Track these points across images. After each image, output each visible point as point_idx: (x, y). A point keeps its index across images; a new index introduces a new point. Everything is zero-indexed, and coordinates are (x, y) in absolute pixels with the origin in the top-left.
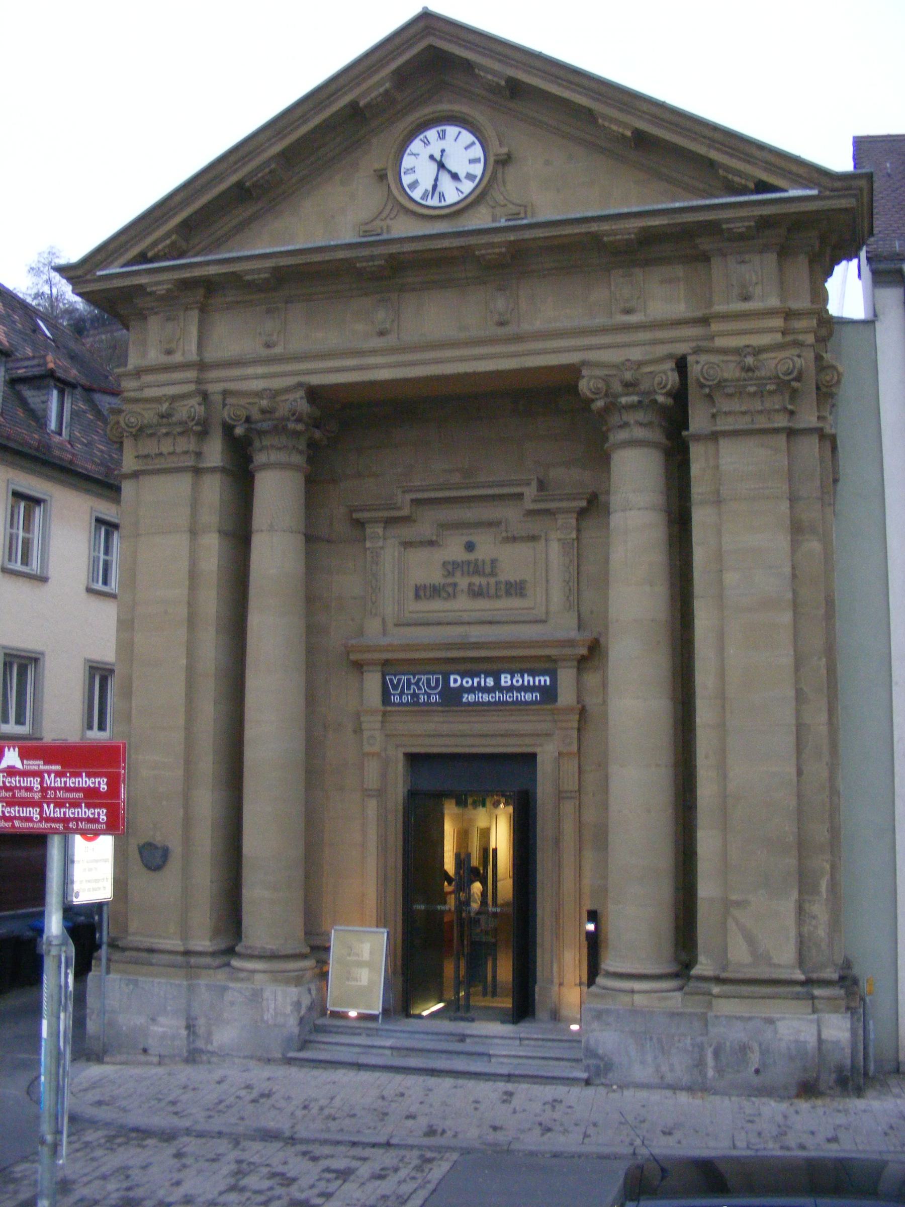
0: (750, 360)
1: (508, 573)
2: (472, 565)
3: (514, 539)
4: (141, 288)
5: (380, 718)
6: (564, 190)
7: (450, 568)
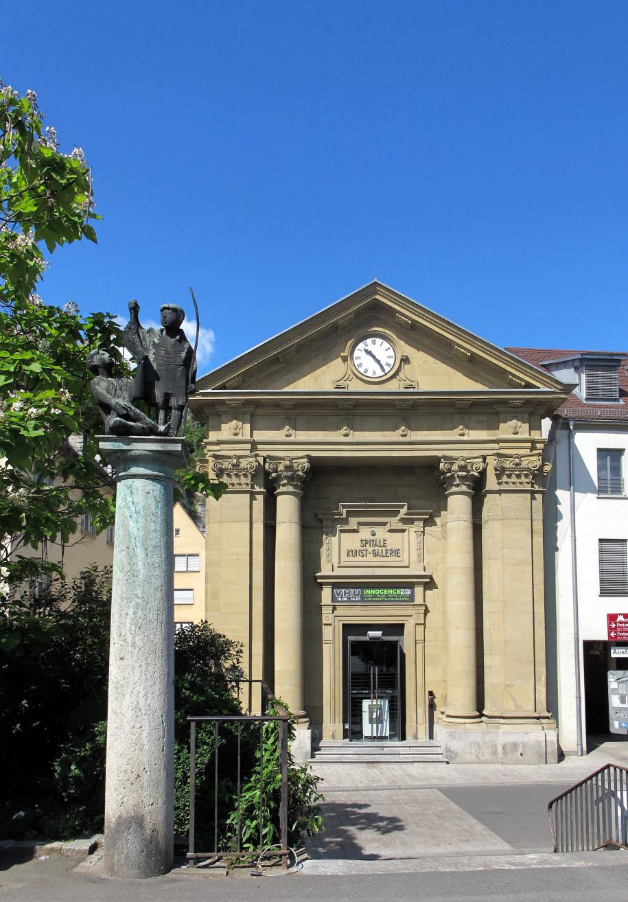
0: (517, 460)
4: (223, 402)
5: (331, 608)
6: (433, 376)
7: (364, 543)
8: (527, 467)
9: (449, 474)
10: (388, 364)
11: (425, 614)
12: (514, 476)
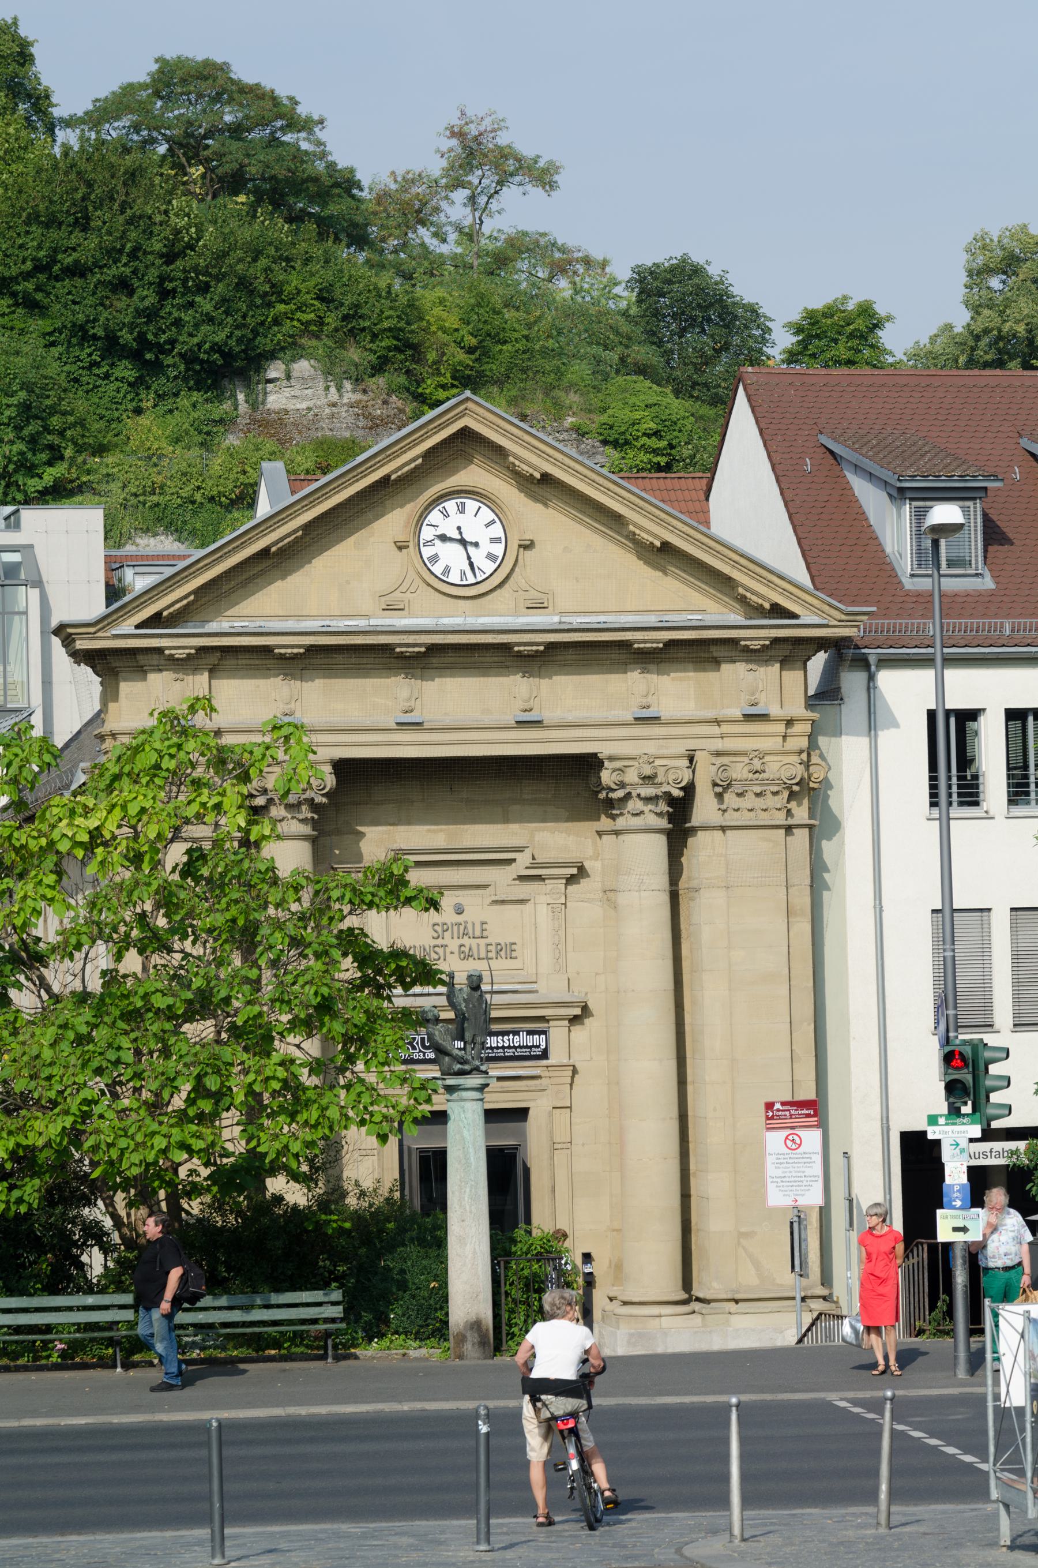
0: (757, 764)
1: (497, 935)
2: (462, 928)
3: (503, 902)
7: (439, 929)
8: (777, 776)
9: (620, 794)
10: (491, 557)
11: (573, 1077)
12: (750, 796)
